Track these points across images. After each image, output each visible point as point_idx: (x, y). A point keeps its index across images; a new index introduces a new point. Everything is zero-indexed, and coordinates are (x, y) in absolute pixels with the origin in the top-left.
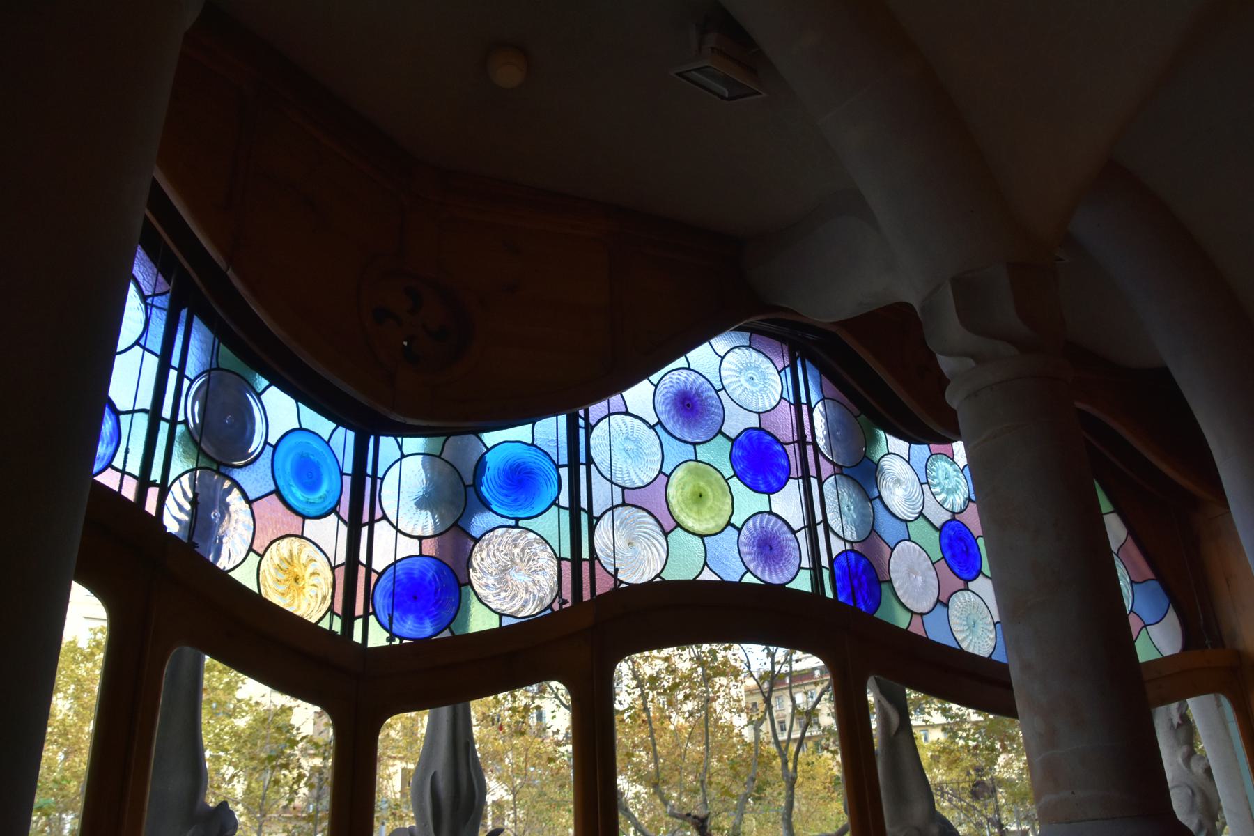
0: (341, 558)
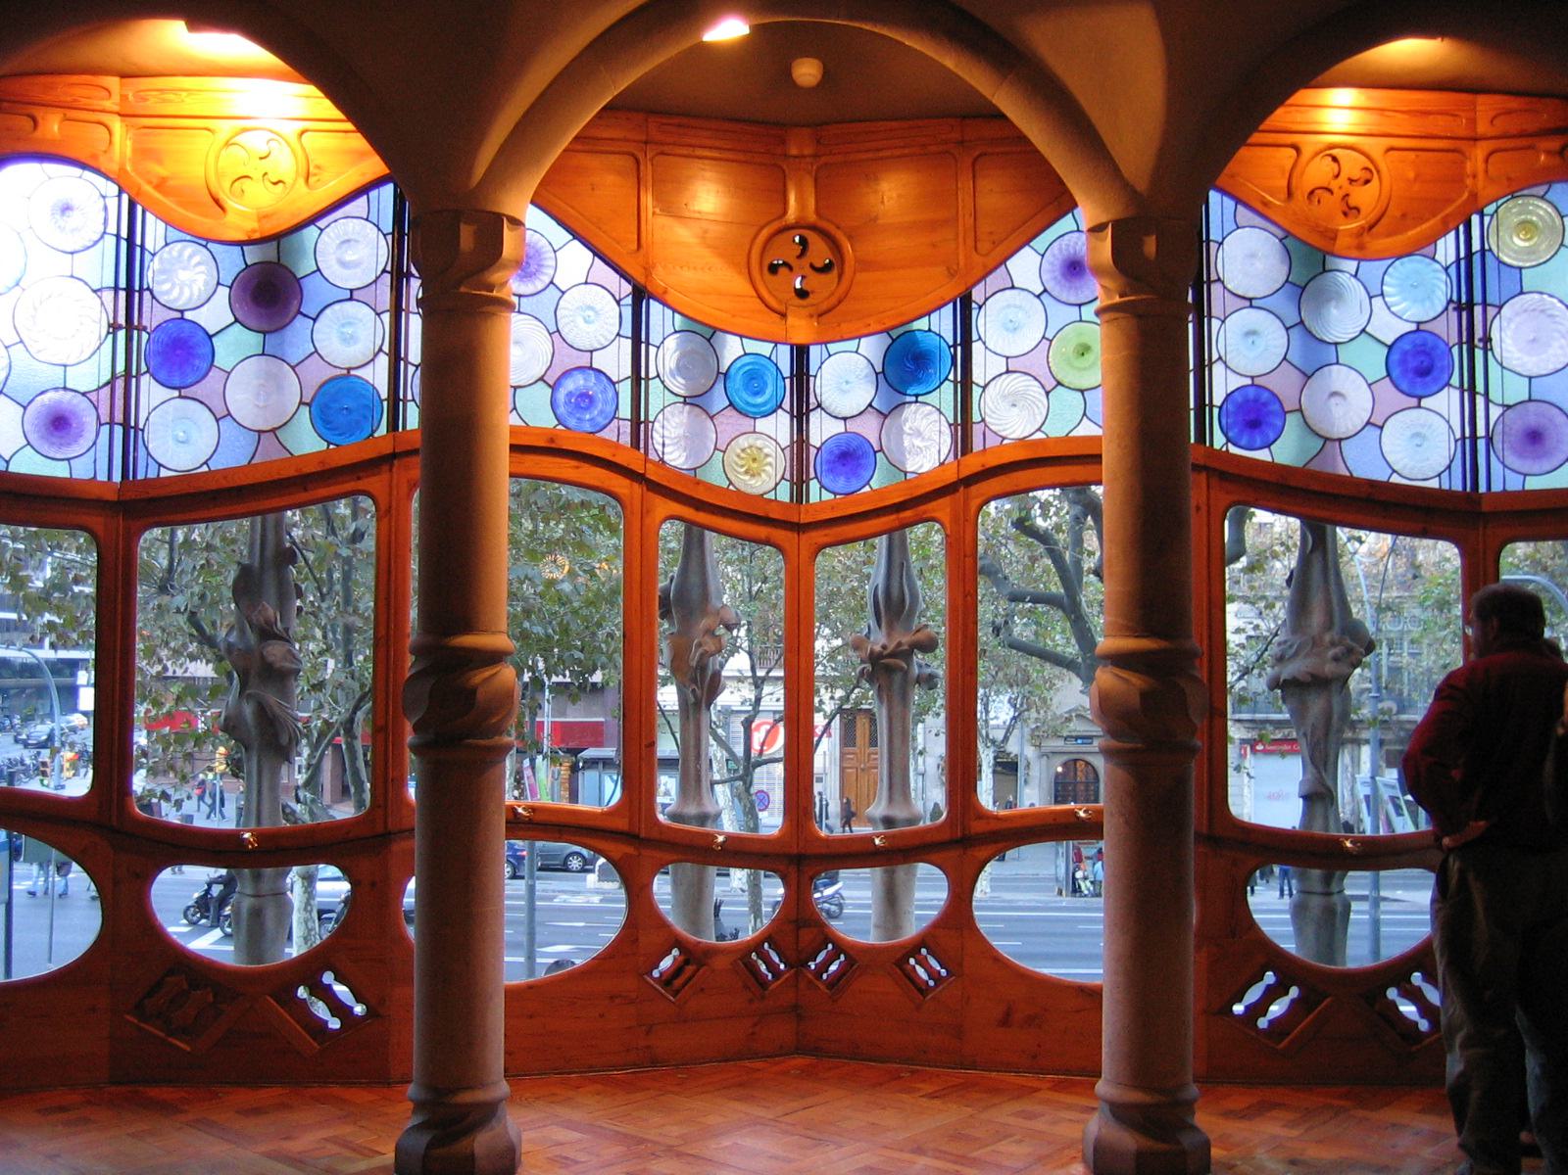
0: (785, 441)
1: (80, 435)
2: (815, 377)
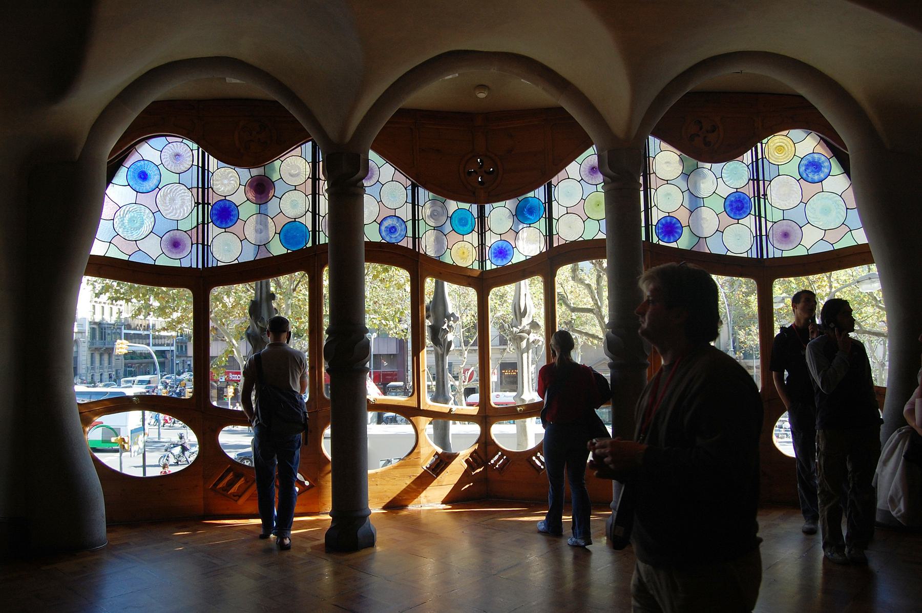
0: (476, 244)
1: (184, 249)
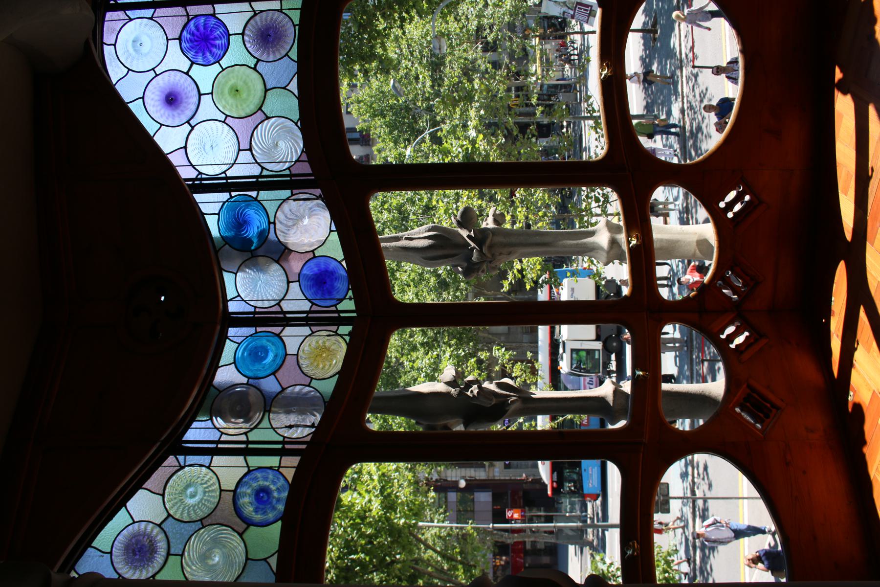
0: (306, 330)
2: (255, 307)
